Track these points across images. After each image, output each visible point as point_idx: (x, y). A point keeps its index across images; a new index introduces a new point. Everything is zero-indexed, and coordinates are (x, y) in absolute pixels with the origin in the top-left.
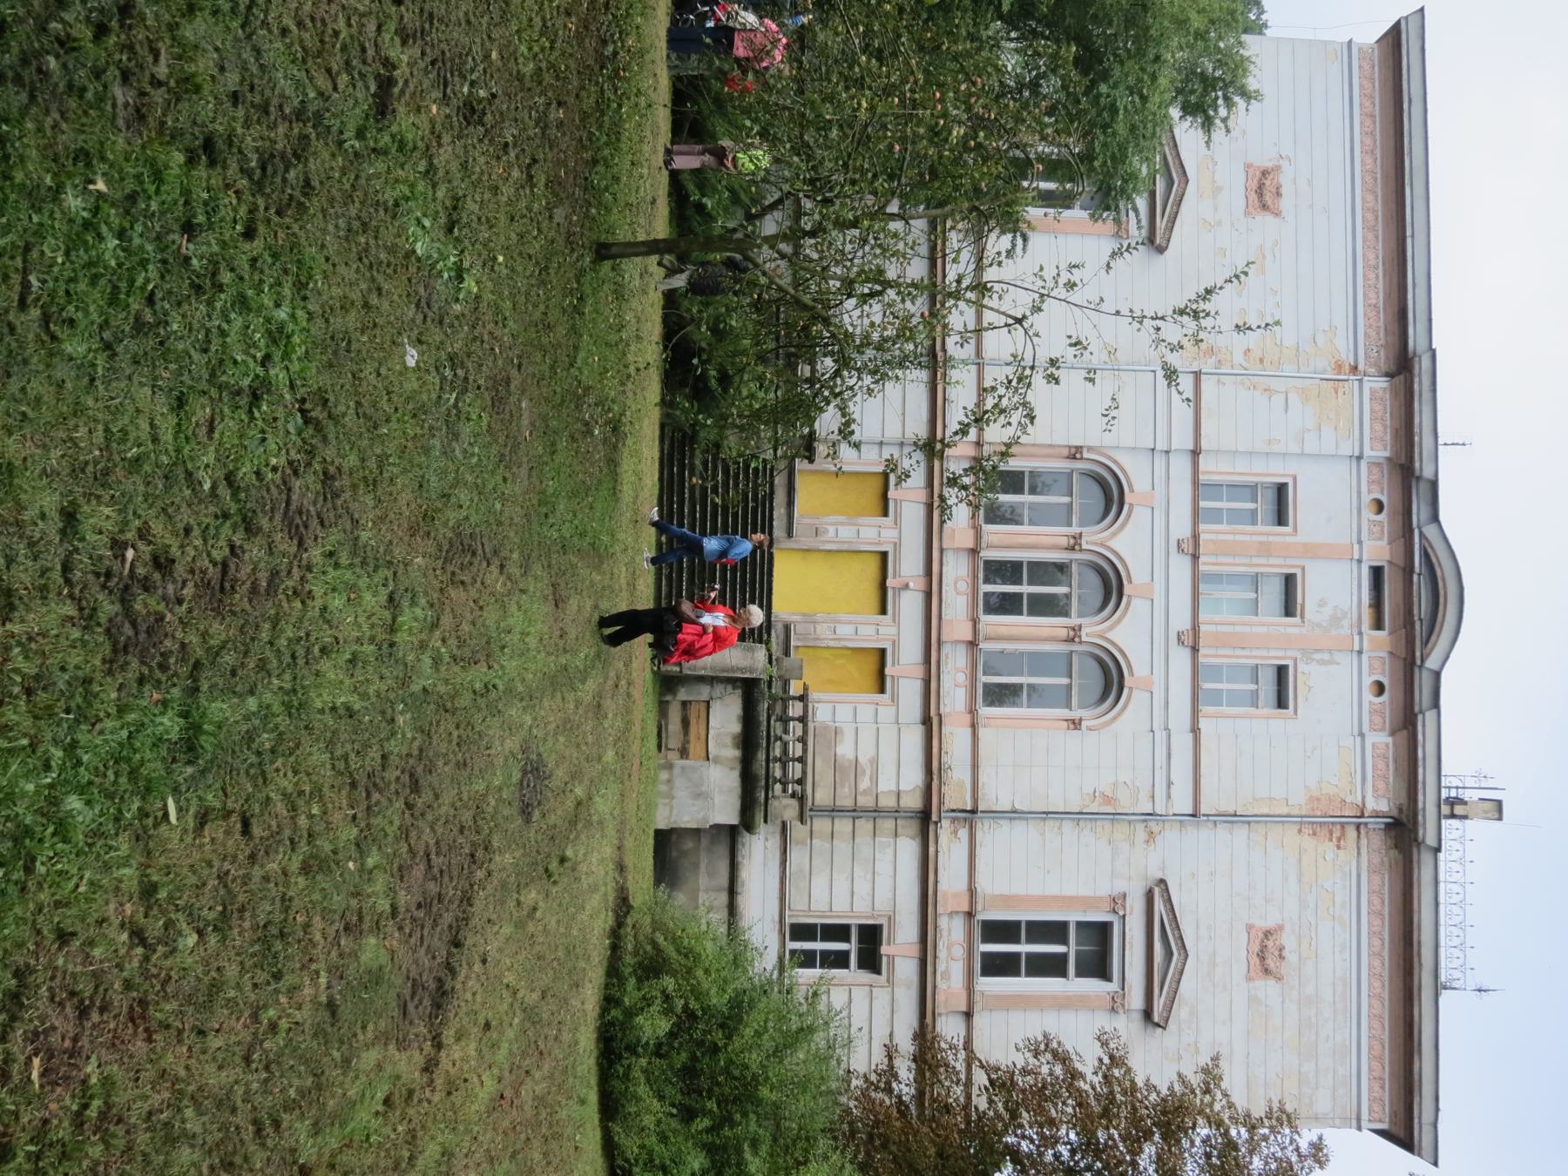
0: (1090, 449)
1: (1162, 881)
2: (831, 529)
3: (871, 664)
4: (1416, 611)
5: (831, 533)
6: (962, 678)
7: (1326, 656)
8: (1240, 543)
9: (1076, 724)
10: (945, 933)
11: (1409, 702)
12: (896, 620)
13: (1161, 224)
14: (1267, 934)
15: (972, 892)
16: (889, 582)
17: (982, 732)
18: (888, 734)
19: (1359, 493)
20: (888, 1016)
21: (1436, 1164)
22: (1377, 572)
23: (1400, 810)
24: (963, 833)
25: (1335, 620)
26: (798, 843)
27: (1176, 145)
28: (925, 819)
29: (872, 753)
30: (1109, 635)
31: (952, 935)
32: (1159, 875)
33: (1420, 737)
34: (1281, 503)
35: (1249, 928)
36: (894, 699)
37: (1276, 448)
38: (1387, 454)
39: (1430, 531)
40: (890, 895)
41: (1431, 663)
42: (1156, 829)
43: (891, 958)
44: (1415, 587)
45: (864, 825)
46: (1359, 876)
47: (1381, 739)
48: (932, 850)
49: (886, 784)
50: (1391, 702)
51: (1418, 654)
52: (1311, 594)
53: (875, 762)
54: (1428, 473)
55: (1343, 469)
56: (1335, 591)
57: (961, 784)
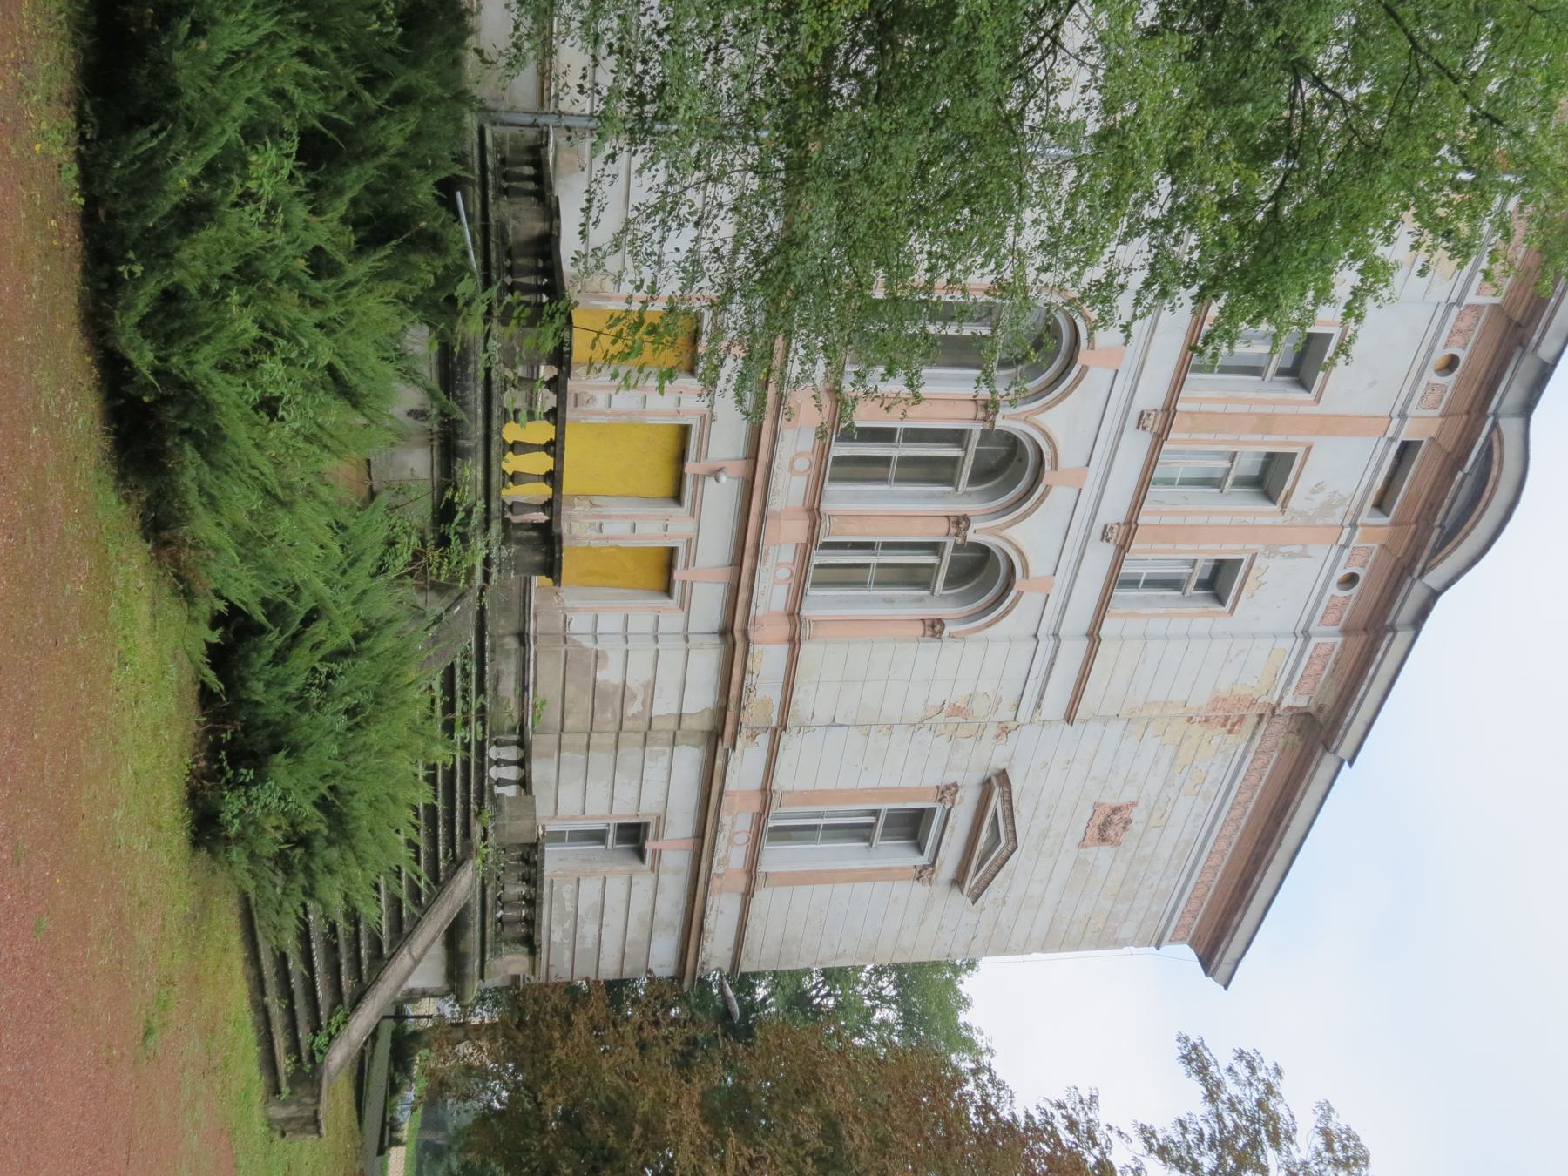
1: (1003, 776)
2: (601, 398)
4: (1440, 515)
5: (601, 403)
6: (784, 573)
9: (935, 627)
10: (727, 828)
11: (1381, 618)
12: (695, 513)
14: (1116, 810)
15: (766, 792)
16: (690, 467)
17: (806, 650)
18: (671, 656)
19: (1431, 349)
20: (650, 895)
21: (1226, 987)
22: (1406, 450)
23: (1320, 709)
25: (1328, 507)
26: (540, 756)
28: (717, 735)
29: (648, 675)
31: (735, 825)
32: (1002, 766)
33: (1379, 655)
35: (1096, 805)
38: (1498, 300)
39: (1510, 427)
40: (662, 798)
41: (1433, 579)
43: (658, 854)
44: (1453, 487)
46: (1243, 758)
47: (1329, 639)
48: (719, 762)
49: (664, 706)
50: (1360, 597)
51: (1419, 566)
52: (1304, 490)
53: (651, 687)
54: (1546, 351)
56: (1340, 471)
57: (767, 703)
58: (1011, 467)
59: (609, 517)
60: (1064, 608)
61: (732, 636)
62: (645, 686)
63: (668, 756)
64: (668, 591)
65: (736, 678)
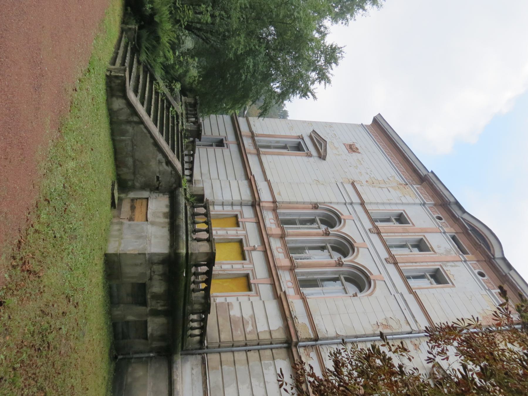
0: (320, 203)
3: (243, 281)
7: (452, 264)
8: (393, 232)
13: (322, 152)
22: (454, 238)
24: (313, 354)
27: (319, 136)
29: (251, 313)
30: (355, 261)
34: (401, 219)
36: (258, 294)
37: (391, 201)
39: (465, 216)
41: (497, 255)
42: (417, 342)
45: (253, 356)
54: (452, 200)
55: (420, 208)
56: (441, 242)
58: (344, 247)
59: (224, 264)
60: (394, 284)
61: (280, 298)
62: (251, 317)
63: (273, 366)
64: (249, 289)
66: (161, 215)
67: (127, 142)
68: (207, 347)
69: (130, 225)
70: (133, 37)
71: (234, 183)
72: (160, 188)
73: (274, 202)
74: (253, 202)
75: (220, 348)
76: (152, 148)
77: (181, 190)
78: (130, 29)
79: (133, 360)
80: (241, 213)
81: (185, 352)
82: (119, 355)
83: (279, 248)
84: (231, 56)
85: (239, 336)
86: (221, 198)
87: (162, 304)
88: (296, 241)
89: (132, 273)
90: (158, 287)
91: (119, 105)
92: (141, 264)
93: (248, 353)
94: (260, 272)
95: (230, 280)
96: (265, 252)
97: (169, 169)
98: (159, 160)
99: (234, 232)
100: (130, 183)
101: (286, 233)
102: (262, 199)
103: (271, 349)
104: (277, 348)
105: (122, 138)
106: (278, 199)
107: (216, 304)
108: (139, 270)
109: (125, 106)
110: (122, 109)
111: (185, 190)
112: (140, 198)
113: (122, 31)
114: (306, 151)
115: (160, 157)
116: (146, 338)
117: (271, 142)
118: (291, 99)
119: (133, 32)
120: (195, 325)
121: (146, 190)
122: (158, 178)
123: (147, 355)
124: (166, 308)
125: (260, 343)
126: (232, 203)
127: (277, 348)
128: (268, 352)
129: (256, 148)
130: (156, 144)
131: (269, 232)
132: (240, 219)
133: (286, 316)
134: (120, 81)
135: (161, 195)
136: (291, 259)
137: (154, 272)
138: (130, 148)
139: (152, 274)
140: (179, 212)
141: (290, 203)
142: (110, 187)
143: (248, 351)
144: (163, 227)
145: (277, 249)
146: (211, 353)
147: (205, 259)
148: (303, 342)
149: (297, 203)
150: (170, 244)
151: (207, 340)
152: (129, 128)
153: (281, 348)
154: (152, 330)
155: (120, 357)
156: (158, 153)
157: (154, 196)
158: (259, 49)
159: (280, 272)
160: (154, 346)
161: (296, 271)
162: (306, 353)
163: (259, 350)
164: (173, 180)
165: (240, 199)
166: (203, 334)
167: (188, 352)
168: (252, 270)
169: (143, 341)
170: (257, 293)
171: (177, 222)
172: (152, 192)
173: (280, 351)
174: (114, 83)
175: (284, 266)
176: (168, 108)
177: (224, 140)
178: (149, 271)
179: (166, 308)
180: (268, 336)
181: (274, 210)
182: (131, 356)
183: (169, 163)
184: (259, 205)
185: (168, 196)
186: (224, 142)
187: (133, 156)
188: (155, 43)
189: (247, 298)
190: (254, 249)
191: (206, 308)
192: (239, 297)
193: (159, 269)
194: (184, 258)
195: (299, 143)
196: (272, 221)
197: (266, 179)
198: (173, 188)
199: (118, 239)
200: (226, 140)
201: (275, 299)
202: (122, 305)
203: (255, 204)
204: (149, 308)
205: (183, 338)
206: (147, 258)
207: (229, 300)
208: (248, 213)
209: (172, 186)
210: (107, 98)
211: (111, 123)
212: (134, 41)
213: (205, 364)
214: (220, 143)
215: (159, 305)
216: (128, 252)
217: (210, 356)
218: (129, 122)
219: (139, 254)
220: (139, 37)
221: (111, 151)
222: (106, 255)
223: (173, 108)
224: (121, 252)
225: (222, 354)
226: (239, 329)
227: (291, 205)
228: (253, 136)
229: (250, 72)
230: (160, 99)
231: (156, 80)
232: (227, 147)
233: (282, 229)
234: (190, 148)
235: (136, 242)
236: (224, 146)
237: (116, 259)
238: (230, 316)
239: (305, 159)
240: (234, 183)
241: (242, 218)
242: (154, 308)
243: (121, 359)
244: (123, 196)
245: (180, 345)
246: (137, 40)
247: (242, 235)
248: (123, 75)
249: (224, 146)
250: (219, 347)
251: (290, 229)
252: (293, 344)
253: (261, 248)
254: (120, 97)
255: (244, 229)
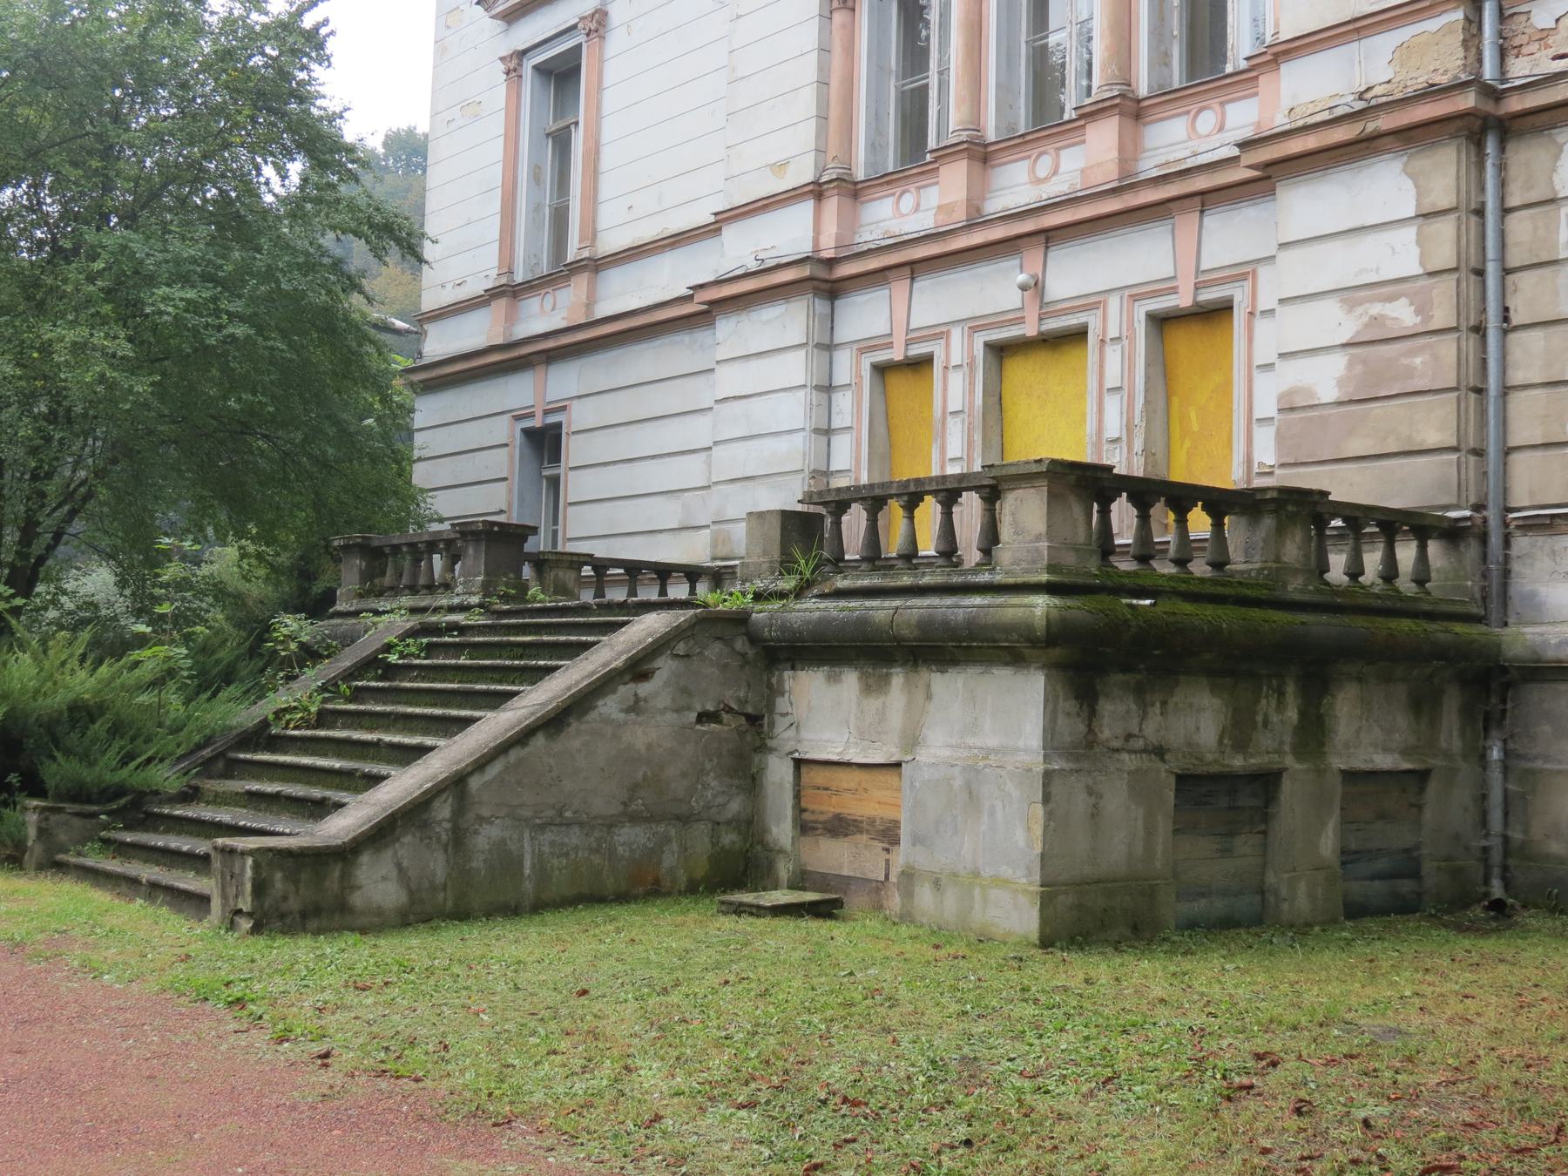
3: (1183, 341)
16: (1030, 330)
36: (1244, 272)
53: (1350, 294)
59: (1100, 430)
61: (1271, 169)
62: (1351, 305)
64: (1219, 312)
65: (1310, 142)
66: (873, 703)
67: (546, 849)
68: (1478, 507)
69: (917, 840)
70: (77, 822)
71: (731, 380)
72: (750, 710)
73: (816, 191)
74: (817, 292)
75: (1484, 450)
76: (574, 738)
77: (761, 614)
78: (42, 832)
79: (1516, 835)
80: (866, 346)
81: (1494, 605)
82: (1487, 895)
83: (1033, 170)
84: (142, 386)
85: (1438, 362)
86: (798, 439)
87: (1273, 702)
88: (1004, 88)
89: (1129, 828)
90: (1197, 722)
91: (384, 879)
92: (1090, 791)
93: (1516, 319)
94: (1143, 261)
95: (1175, 401)
96: (1050, 237)
97: (665, 667)
98: (628, 711)
99: (956, 382)
100: (729, 839)
101: (964, 136)
102: (804, 248)
103: (1505, 211)
104: (1502, 184)
105: (527, 872)
106: (803, 173)
107: (1282, 465)
108: (1117, 800)
109: (388, 855)
110: (399, 866)
111: (758, 597)
112: (797, 796)
113: (54, 865)
114: (581, 39)
115: (609, 706)
116: (1422, 776)
117: (538, 208)
118: (333, 106)
119: (54, 818)
120: (1373, 560)
121: (762, 769)
122: (703, 717)
123: (1495, 776)
124: (1290, 689)
125: (1473, 263)
126: (818, 388)
127: (1502, 184)
128: (1520, 227)
129: (567, 277)
130: (555, 721)
131: (960, 216)
132: (897, 354)
133: (1354, 140)
134: (279, 875)
135: (782, 704)
136: (1089, 115)
137: (1129, 737)
138: (574, 837)
139: (1140, 744)
140: (863, 622)
141: (822, 118)
142: (746, 924)
143: (1506, 319)
144: (929, 697)
145: (1039, 181)
146: (1505, 491)
147: (1077, 510)
148: (1480, 61)
149: (823, 83)
150: (1007, 664)
151: (1447, 508)
152: (485, 838)
153: (1502, 167)
154: (1386, 750)
155: (1497, 890)
156: (593, 715)
157: (791, 733)
158: (104, 255)
159: (1149, 167)
160: (1457, 744)
161: (1143, 91)
162: (1534, 47)
163: (1507, 271)
164: (715, 650)
165: (802, 353)
166: (1420, 525)
167: (1497, 594)
168: (1135, 298)
169: (1433, 787)
170: (1242, 277)
171: (906, 632)
172: (770, 743)
173: (1515, 170)
174: (285, 898)
175: (1121, 149)
176: (390, 671)
177: (527, 424)
178: (1125, 756)
179: (1290, 689)
180: (1445, 229)
181: (854, 191)
182: (1495, 842)
183: (637, 668)
184: (831, 263)
185: (787, 674)
186: (536, 423)
187: (611, 824)
188: (99, 727)
189: (1261, 325)
190: (1035, 287)
191: (1301, 509)
192: (1258, 361)
193: (1116, 714)
194: (1069, 602)
195: (542, 70)
196: (908, 201)
197: (710, 230)
198: (751, 652)
199: (977, 891)
200: (531, 415)
201: (1272, 192)
202: (1271, 878)
203: (825, 282)
204: (1289, 761)
205: (1431, 616)
206: (1072, 765)
207: (1266, 405)
208: (866, 316)
209: (743, 655)
210: (352, 930)
211: (461, 914)
212: (94, 815)
213: (1553, 516)
214: (544, 442)
215: (1275, 718)
216: (1038, 848)
217: (1521, 495)
218: (458, 840)
219: (1046, 799)
220: (78, 794)
221: (586, 915)
222: (1046, 942)
223: (388, 648)
224: (1037, 878)
225: (1513, 441)
226: (1405, 361)
227: (834, 113)
228: (509, 292)
229: (215, 299)
230: (352, 707)
231: (265, 724)
232: (564, 408)
233: (946, 153)
234: (568, 577)
235: (992, 814)
236: (559, 426)
237: (1065, 900)
238: (1340, 403)
239: (616, 41)
240: (731, 380)
241: (890, 345)
242: (1288, 739)
243: (1507, 886)
244: (784, 870)
245: (1459, 628)
246: (89, 801)
247: (971, 345)
248: (250, 861)
249: (559, 426)
250: (1479, 453)
251: (949, 118)
252: (1489, 107)
253: (1033, 257)
254: (346, 876)
255: (939, 333)
